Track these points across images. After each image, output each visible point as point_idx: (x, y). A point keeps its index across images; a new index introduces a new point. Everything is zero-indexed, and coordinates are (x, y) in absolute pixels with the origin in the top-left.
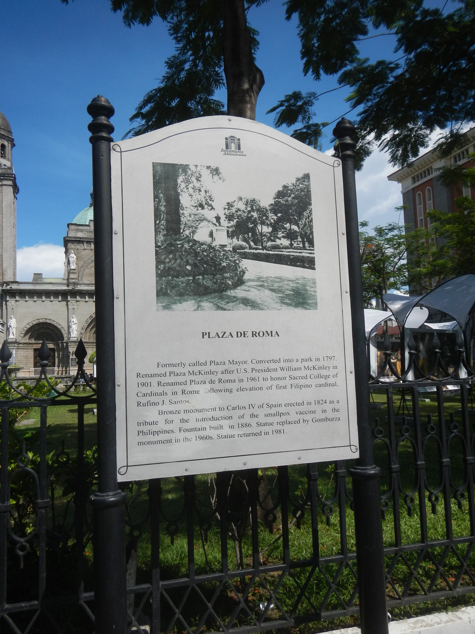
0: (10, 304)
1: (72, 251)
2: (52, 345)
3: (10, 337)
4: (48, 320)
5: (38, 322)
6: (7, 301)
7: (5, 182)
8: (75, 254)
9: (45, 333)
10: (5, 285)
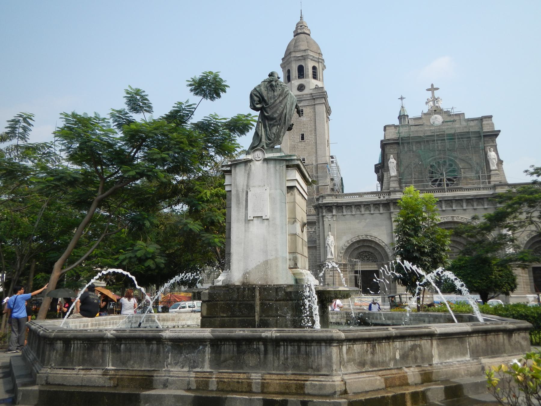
1: (392, 156)
2: (376, 266)
4: (369, 237)
6: (323, 216)
7: (317, 102)
9: (366, 252)
10: (321, 199)
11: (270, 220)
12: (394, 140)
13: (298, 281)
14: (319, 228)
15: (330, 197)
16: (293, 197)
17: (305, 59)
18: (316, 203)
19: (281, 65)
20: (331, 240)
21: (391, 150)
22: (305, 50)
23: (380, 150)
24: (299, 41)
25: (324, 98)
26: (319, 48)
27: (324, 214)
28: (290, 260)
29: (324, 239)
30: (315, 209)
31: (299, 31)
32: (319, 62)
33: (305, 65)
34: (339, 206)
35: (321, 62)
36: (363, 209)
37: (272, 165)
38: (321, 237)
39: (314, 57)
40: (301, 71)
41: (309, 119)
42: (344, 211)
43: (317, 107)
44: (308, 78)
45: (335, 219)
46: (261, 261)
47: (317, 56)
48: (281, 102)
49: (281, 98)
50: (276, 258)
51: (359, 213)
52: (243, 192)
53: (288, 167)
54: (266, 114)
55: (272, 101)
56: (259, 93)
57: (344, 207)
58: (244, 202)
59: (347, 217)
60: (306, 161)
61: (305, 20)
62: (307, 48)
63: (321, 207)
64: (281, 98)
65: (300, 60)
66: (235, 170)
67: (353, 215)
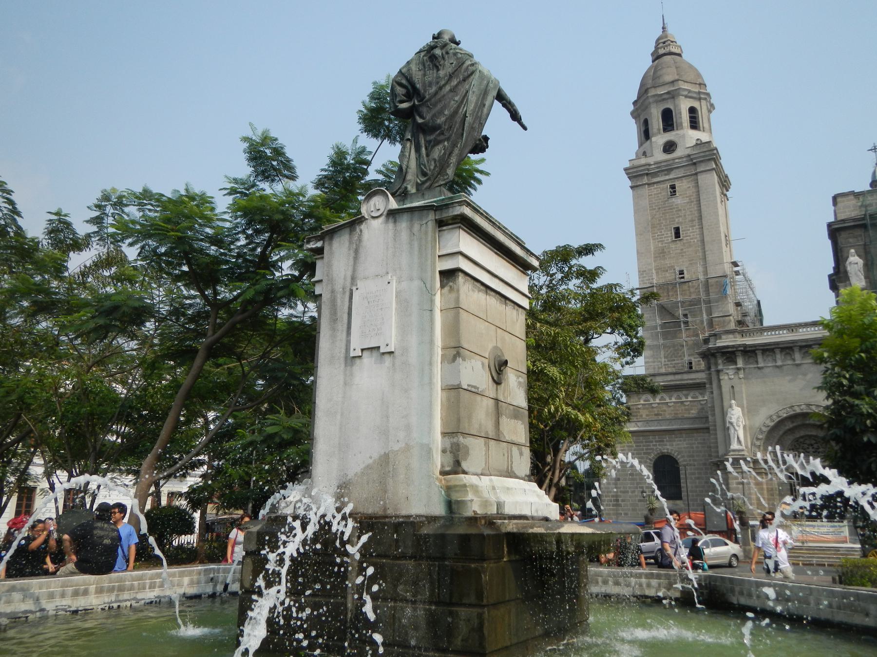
0: (726, 377)
3: (732, 447)
4: (813, 408)
5: (792, 413)
6: (718, 372)
8: (859, 256)
9: (810, 436)
10: (712, 339)
11: (396, 354)
12: (854, 220)
13: (454, 506)
14: (712, 393)
15: (731, 336)
16: (453, 295)
17: (673, 98)
18: (704, 348)
19: (632, 114)
20: (736, 414)
21: (851, 240)
22: (673, 82)
23: (828, 243)
24: (662, 68)
25: (714, 160)
26: (699, 75)
27: (720, 367)
28: (444, 451)
29: (724, 414)
30: (703, 358)
31: (661, 51)
32: (700, 99)
33: (675, 106)
34: (749, 351)
35: (705, 99)
36: (797, 356)
37: (403, 224)
38: (717, 410)
39: (690, 91)
40: (669, 120)
41: (687, 200)
42: (760, 359)
43: (700, 177)
44: (682, 128)
45: (741, 376)
46: (376, 456)
47: (696, 89)
48: (453, 90)
49: (454, 82)
50: (408, 448)
51: (790, 362)
52: (344, 293)
53: (441, 224)
54: (420, 121)
55: (433, 90)
56: (406, 78)
57: (759, 353)
58: (346, 316)
59: (767, 371)
60: (686, 275)
61: (670, 30)
62: (677, 77)
63: (713, 355)
64: (454, 82)
65: (664, 100)
66: (330, 244)
67: (777, 367)
